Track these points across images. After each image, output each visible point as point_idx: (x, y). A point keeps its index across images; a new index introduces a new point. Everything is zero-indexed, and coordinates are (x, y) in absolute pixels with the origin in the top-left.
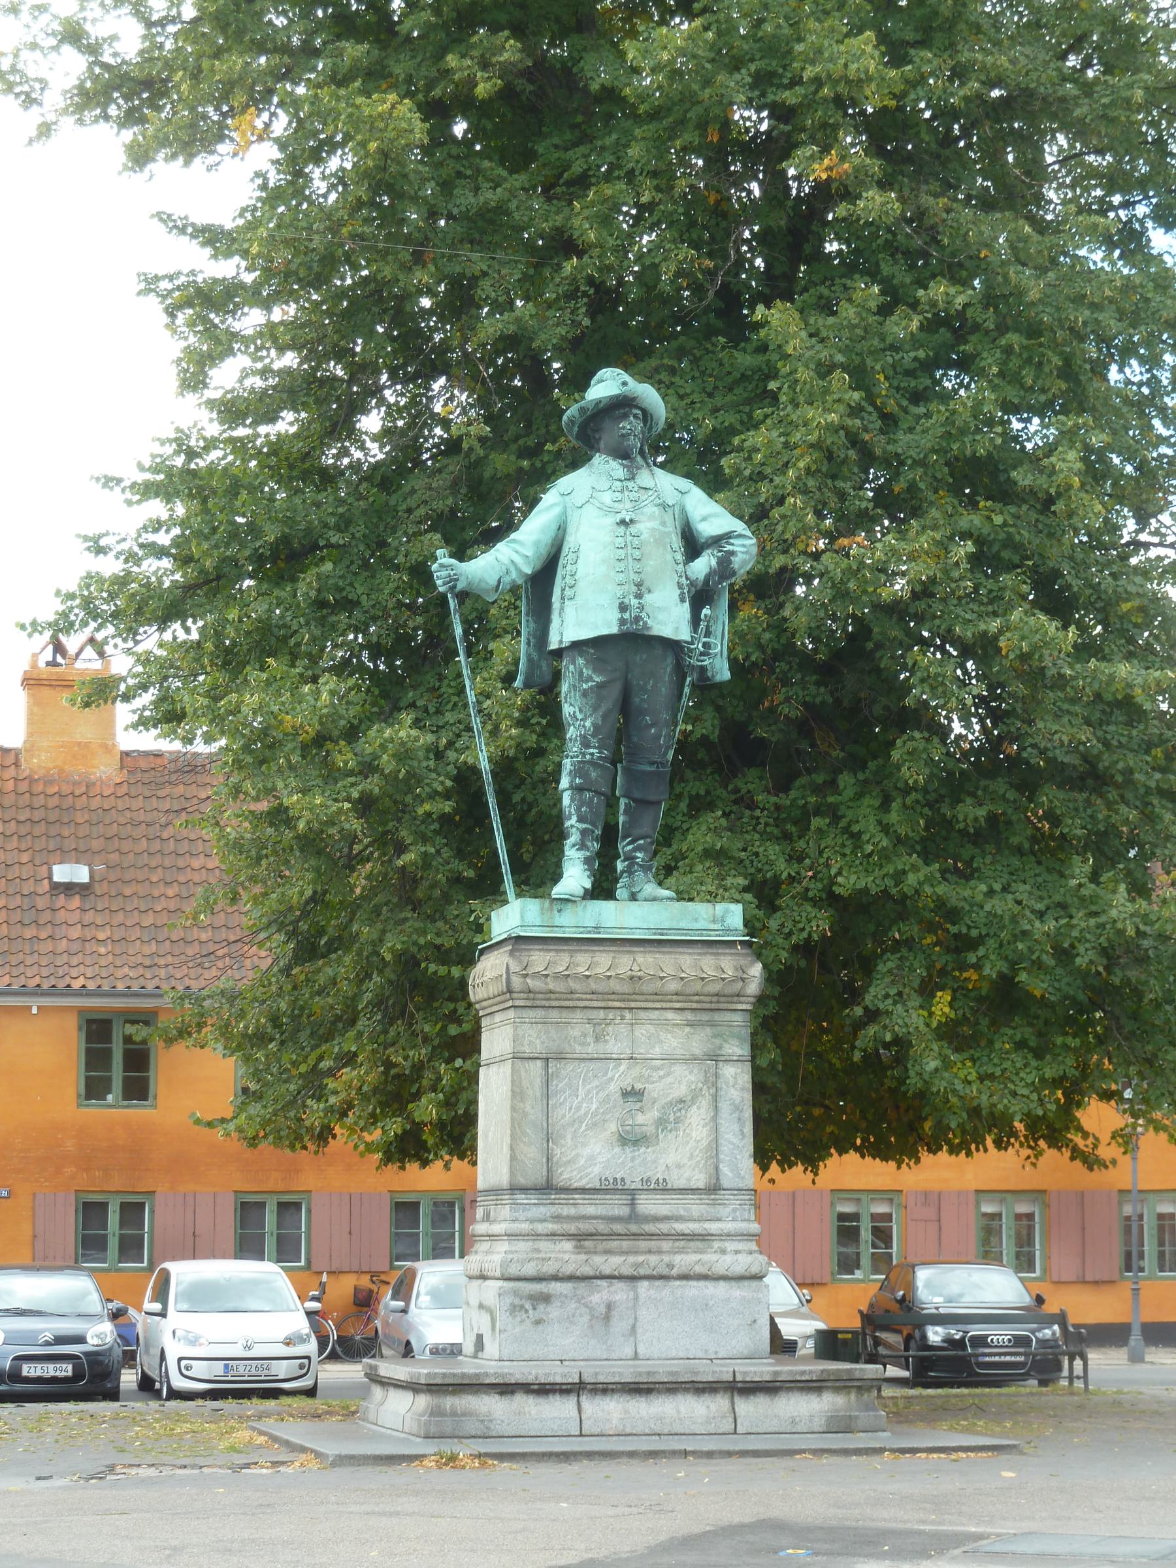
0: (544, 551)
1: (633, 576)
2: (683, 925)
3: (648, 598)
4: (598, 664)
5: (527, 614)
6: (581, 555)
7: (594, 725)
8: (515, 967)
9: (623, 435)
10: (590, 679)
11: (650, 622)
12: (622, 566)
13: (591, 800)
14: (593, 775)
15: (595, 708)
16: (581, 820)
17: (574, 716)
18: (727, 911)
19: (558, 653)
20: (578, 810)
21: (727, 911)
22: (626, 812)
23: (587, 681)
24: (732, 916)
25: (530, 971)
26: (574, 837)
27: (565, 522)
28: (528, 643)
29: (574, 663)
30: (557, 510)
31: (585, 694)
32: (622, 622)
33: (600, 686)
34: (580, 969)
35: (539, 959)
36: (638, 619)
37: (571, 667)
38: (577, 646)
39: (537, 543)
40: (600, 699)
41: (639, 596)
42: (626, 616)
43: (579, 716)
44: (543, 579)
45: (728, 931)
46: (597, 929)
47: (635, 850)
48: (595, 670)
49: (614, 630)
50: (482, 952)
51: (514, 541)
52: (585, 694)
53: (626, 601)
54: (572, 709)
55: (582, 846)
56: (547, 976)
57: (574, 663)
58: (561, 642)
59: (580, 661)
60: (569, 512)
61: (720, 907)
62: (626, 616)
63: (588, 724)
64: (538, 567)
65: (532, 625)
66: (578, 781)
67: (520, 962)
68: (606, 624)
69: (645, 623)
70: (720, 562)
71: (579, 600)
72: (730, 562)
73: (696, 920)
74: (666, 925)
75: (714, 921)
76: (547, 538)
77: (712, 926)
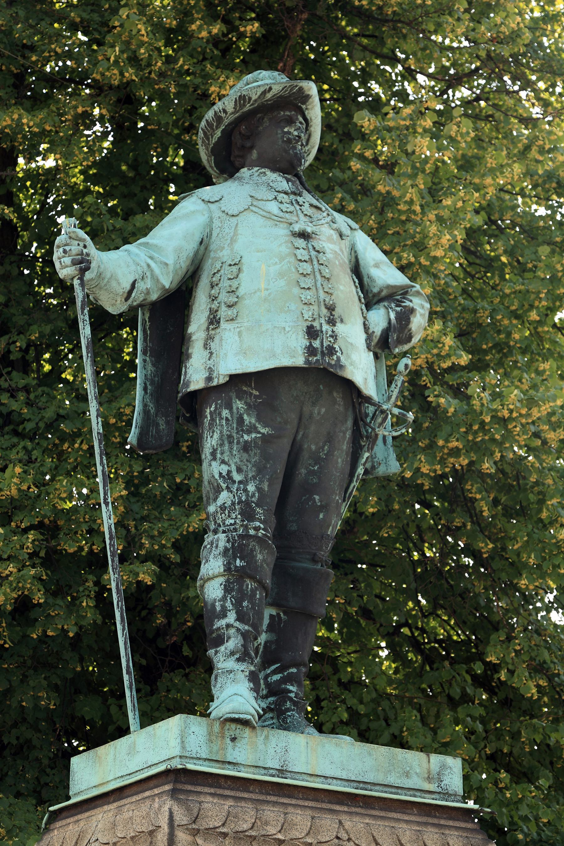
0: (184, 264)
1: (322, 295)
2: (392, 780)
3: (340, 328)
4: (264, 409)
5: (144, 353)
6: (244, 268)
7: (259, 489)
8: (181, 817)
9: (289, 141)
10: (252, 429)
11: (342, 358)
12: (308, 282)
13: (253, 591)
14: (259, 557)
15: (260, 470)
16: (240, 618)
17: (229, 477)
18: (443, 766)
19: (195, 402)
20: (238, 605)
21: (443, 766)
22: (271, 628)
23: (249, 432)
24: (451, 771)
25: (203, 824)
26: (233, 643)
27: (209, 235)
28: (145, 389)
29: (229, 407)
30: (202, 219)
31: (246, 447)
32: (311, 351)
33: (265, 439)
34: (271, 830)
35: (214, 809)
36: (331, 351)
37: (225, 413)
38: (236, 380)
39: (178, 250)
40: (265, 456)
41: (332, 322)
42: (316, 344)
43: (237, 477)
44: (171, 312)
45: (446, 795)
46: (281, 772)
47: (284, 680)
48: (259, 419)
49: (299, 361)
50: (55, 816)
51: (146, 245)
52: (246, 447)
53: (316, 324)
54: (224, 469)
55: (244, 656)
56: (225, 835)
57: (229, 407)
58: (209, 379)
59: (239, 405)
60: (216, 223)
61: (436, 759)
62: (316, 344)
63: (251, 488)
64: (174, 285)
65: (150, 367)
66: (238, 562)
67: (188, 809)
68: (286, 350)
69: (339, 359)
70: (399, 317)
71: (245, 322)
72: (408, 321)
73: (407, 775)
74: (369, 778)
75: (429, 779)
76: (190, 247)
77: (427, 786)
